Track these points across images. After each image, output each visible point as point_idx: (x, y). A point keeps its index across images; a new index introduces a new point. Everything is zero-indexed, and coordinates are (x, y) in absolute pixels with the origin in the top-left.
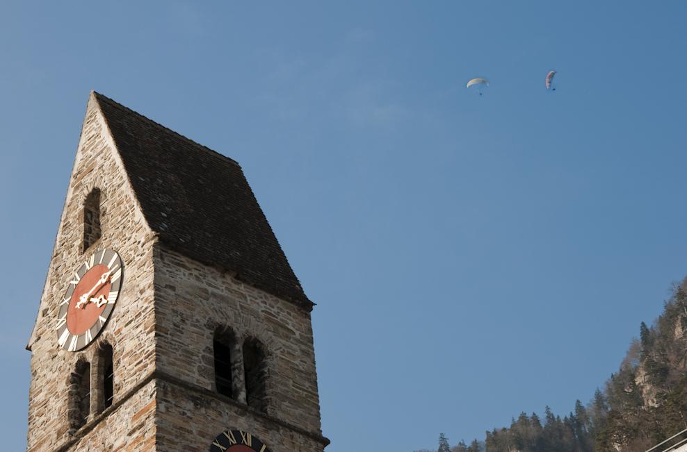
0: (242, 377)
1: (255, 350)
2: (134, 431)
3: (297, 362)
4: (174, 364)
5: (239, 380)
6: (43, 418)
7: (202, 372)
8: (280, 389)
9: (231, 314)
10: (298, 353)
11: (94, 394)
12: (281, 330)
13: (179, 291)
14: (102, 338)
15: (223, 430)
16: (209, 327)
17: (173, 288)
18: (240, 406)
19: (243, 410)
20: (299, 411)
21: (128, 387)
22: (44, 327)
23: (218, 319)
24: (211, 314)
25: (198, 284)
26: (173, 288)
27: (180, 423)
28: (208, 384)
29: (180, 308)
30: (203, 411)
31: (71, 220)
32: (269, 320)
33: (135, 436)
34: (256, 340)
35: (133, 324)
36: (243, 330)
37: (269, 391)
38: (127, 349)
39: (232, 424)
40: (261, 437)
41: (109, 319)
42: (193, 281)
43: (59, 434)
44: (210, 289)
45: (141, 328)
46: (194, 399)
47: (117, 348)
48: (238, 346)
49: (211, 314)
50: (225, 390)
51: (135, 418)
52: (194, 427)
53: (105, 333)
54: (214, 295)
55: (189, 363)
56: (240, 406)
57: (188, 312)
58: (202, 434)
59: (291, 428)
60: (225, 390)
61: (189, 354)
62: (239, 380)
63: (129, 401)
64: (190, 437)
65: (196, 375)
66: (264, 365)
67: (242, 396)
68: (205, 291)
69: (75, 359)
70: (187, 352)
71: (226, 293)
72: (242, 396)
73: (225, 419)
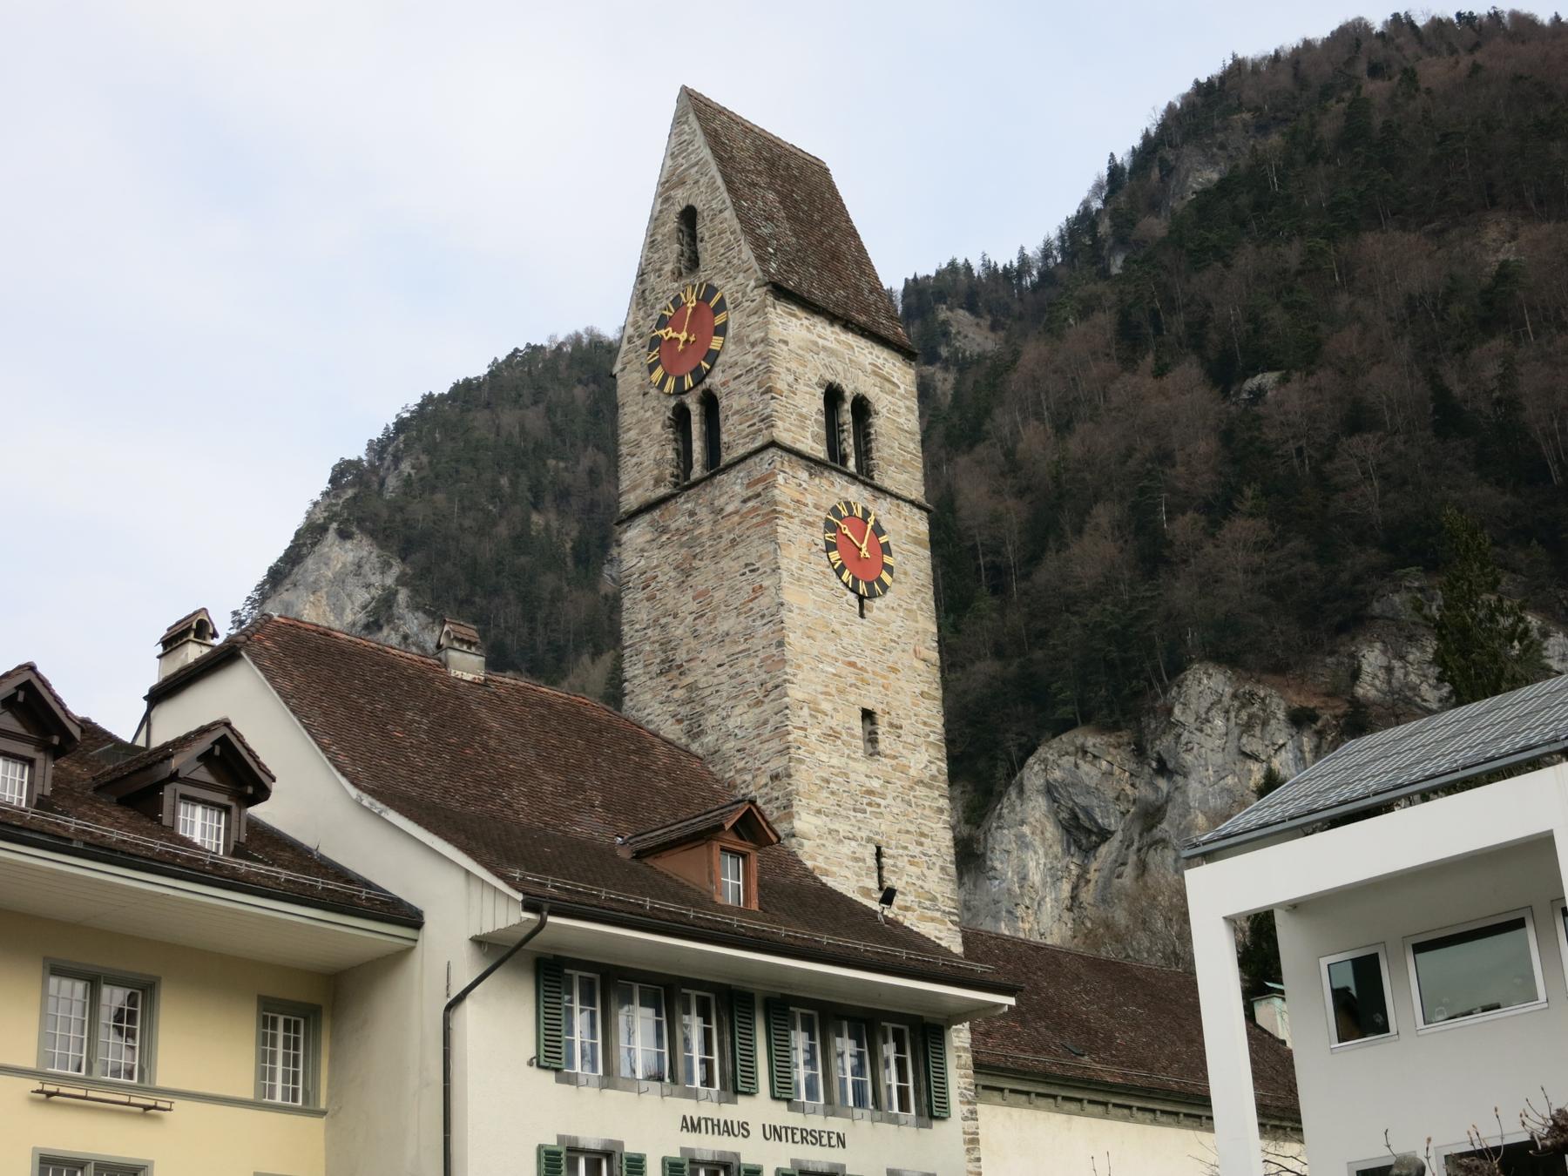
0: (851, 441)
1: (862, 408)
2: (749, 499)
3: (902, 420)
4: (788, 430)
5: (849, 445)
6: (634, 460)
7: (815, 437)
8: (886, 452)
9: (840, 368)
10: (903, 410)
11: (697, 446)
12: (887, 385)
13: (791, 346)
14: (703, 387)
15: (835, 502)
16: (821, 386)
17: (786, 343)
18: (850, 475)
19: (853, 478)
20: (905, 476)
21: (741, 451)
22: (633, 355)
23: (829, 377)
24: (823, 371)
25: (809, 336)
26: (786, 343)
27: (797, 496)
28: (821, 452)
29: (793, 366)
30: (817, 480)
31: (659, 238)
32: (875, 373)
33: (750, 504)
34: (864, 398)
35: (743, 379)
36: (851, 387)
37: (875, 455)
38: (736, 407)
39: (843, 494)
40: (870, 508)
41: (712, 366)
42: (804, 332)
43: (658, 482)
44: (821, 342)
45: (752, 386)
46: (809, 469)
47: (723, 403)
48: (847, 406)
49: (823, 371)
50: (836, 459)
51: (749, 486)
52: (809, 499)
53: (708, 380)
54: (825, 348)
55: (803, 428)
56: (850, 475)
57: (801, 369)
58: (817, 507)
59: (898, 497)
60: (836, 459)
61: (803, 417)
62: (849, 445)
63: (742, 466)
64: (805, 509)
65: (810, 442)
66: (870, 426)
67: (852, 463)
68: (816, 344)
69: (673, 402)
70: (800, 415)
71: (834, 346)
72: (852, 463)
73: (836, 490)
